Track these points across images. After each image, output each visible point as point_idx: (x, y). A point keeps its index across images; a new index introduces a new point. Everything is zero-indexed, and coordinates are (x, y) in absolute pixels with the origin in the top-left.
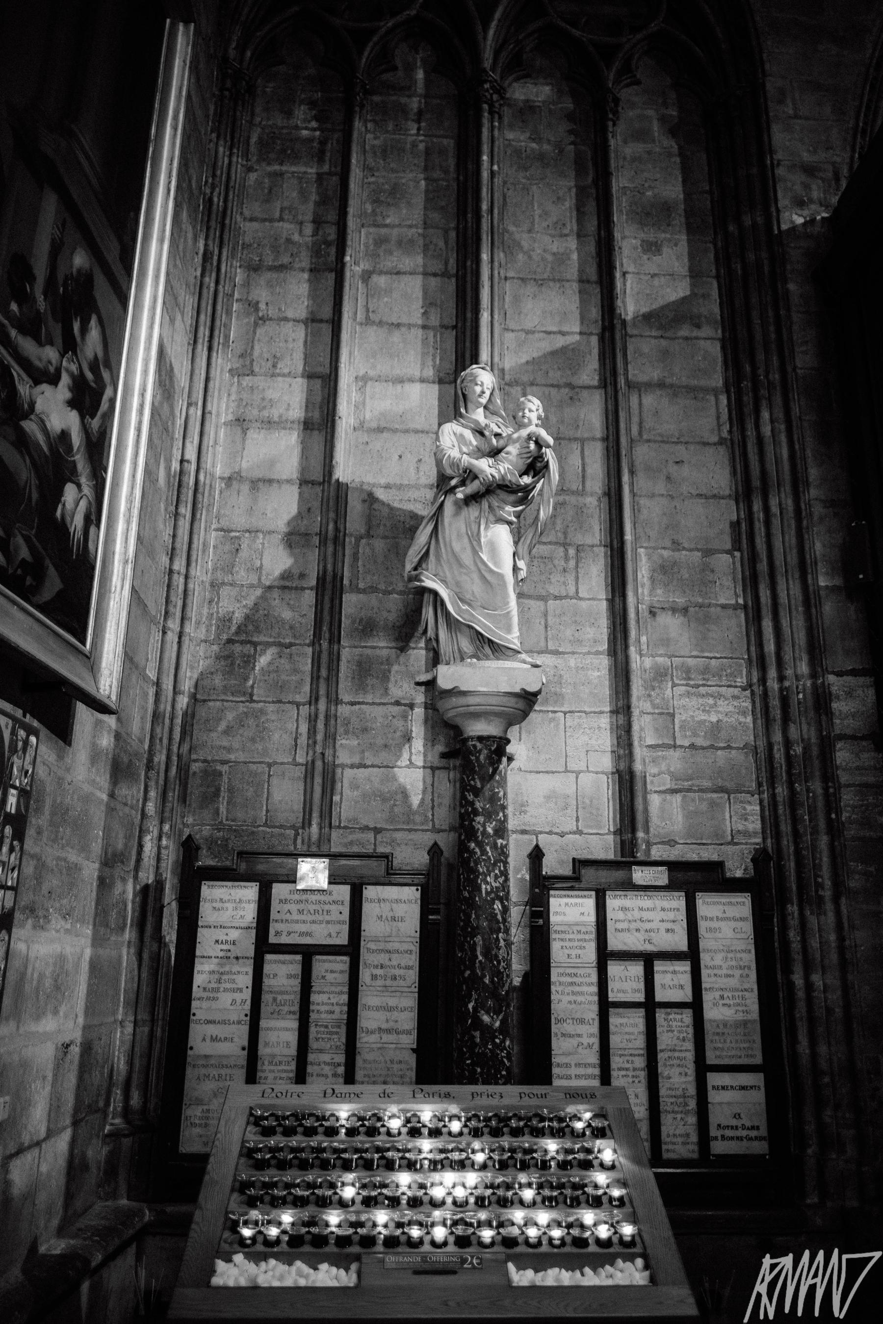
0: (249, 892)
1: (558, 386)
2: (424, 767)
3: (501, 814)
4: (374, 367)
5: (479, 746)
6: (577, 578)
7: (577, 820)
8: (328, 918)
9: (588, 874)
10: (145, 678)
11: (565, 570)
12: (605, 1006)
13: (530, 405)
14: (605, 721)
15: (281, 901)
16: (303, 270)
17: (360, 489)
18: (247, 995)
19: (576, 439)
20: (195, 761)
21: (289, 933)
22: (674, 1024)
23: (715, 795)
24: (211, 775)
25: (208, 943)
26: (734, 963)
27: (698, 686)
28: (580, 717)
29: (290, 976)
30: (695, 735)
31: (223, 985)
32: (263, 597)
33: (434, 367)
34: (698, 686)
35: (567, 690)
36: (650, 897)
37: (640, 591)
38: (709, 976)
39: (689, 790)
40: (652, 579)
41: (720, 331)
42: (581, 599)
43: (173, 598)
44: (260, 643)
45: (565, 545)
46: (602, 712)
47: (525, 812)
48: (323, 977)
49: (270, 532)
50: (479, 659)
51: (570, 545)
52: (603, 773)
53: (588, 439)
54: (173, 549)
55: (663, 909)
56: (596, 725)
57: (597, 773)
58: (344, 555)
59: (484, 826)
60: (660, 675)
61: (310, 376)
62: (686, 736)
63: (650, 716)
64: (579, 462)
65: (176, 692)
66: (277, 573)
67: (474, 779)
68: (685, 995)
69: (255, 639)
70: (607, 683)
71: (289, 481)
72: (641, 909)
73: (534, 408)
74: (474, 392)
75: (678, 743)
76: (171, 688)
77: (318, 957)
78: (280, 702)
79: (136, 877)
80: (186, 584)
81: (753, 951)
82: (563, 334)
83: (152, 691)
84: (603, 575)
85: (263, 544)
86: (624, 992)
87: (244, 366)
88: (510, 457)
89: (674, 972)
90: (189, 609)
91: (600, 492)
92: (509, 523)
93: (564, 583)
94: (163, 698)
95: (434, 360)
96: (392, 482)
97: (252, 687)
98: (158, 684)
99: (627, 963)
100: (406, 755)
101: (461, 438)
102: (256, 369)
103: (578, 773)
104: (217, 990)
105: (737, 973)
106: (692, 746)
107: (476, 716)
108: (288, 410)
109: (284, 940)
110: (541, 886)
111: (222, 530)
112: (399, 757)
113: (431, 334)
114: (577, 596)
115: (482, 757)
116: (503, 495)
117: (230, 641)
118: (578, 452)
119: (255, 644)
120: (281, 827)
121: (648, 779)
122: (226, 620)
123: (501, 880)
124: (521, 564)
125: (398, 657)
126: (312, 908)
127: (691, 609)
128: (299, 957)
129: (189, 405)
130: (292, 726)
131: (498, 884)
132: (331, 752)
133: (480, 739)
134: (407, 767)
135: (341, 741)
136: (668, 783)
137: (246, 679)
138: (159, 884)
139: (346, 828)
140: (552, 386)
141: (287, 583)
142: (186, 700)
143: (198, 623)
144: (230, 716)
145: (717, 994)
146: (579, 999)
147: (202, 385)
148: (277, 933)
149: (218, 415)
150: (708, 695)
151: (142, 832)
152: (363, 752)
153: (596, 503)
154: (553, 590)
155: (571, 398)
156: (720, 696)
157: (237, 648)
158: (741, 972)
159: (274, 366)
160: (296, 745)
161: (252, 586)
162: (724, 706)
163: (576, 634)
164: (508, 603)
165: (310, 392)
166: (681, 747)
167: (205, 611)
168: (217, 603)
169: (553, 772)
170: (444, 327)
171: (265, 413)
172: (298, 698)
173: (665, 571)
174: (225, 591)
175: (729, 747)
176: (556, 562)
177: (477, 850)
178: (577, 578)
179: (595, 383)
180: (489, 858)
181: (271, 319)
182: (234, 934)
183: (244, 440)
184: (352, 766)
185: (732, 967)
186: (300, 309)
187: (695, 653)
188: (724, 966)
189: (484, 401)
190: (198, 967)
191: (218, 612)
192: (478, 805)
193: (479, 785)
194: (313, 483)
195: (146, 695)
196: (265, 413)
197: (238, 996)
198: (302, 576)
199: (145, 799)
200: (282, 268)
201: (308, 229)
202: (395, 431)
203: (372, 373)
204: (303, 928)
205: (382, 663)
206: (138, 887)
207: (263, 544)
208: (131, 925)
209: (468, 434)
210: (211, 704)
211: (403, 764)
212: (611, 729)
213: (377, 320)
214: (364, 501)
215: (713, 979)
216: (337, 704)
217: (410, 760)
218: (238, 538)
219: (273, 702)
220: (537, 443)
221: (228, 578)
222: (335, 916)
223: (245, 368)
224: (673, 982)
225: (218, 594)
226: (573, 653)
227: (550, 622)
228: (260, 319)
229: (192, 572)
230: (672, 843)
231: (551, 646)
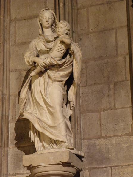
1: (104, 4)
6: (115, 99)
19: (112, 29)
28: (119, 169)
42: (116, 109)
46: (129, 165)
64: (114, 40)
114: (115, 108)
118: (114, 35)
140: (101, 4)
178: (115, 99)
226: (114, 136)
227: (102, 123)
231: (104, 134)
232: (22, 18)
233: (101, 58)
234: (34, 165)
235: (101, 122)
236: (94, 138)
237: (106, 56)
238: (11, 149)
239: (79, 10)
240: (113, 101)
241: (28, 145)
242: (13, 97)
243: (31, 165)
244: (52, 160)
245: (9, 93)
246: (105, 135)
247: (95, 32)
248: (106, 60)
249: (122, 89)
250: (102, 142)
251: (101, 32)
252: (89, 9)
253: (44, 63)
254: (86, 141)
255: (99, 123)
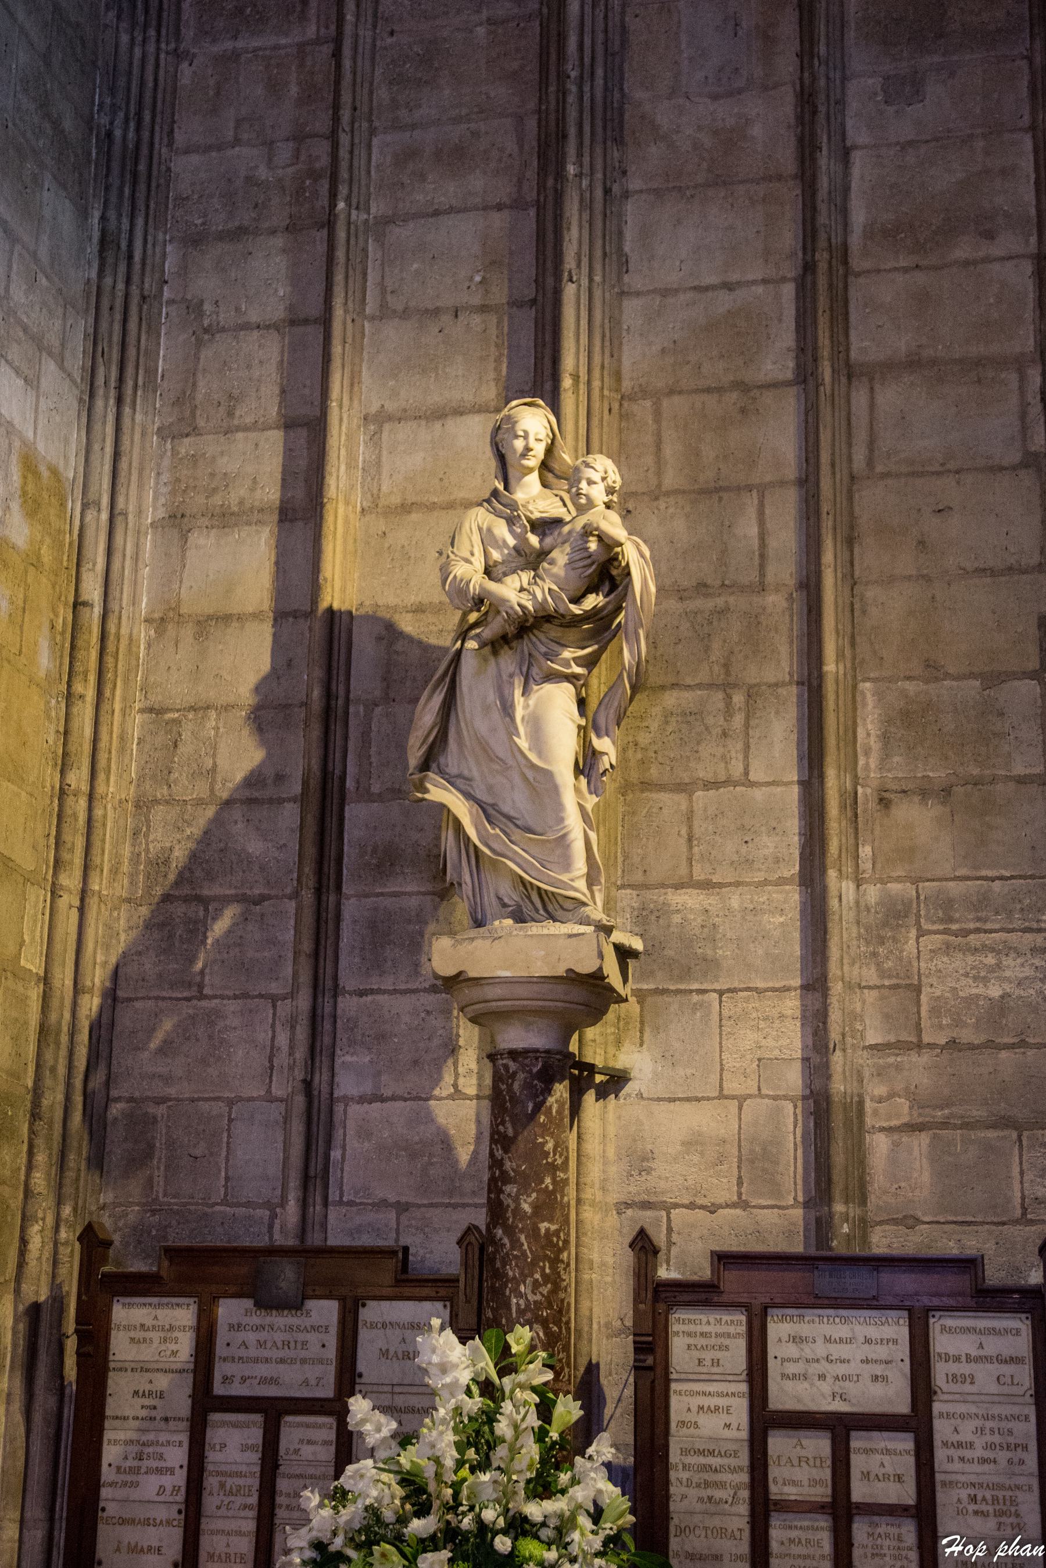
0: (182, 1315)
1: (720, 390)
2: (478, 1097)
3: (548, 1180)
4: (394, 394)
5: (513, 1066)
7: (740, 1183)
8: (303, 1354)
9: (732, 1279)
10: (20, 974)
11: (725, 734)
12: (763, 1507)
13: (589, 473)
14: (792, 1004)
15: (231, 1327)
16: (273, 232)
17: (372, 619)
18: (180, 1478)
19: (749, 488)
20: (118, 1099)
21: (244, 1379)
22: (887, 1543)
23: (991, 1134)
24: (141, 1124)
25: (122, 1397)
26: (997, 1439)
27: (966, 933)
28: (747, 1000)
29: (245, 1448)
30: (958, 1023)
31: (146, 1463)
32: (217, 821)
33: (497, 380)
34: (966, 933)
35: (725, 952)
36: (846, 1320)
37: (861, 762)
38: (950, 1459)
39: (944, 1125)
40: (885, 738)
41: (1033, 240)
42: (752, 784)
43: (67, 837)
44: (215, 898)
45: (727, 687)
46: (787, 989)
47: (649, 1171)
48: (297, 1451)
49: (227, 708)
50: (520, 918)
51: (735, 686)
52: (785, 1097)
53: (772, 484)
54: (65, 754)
55: (868, 1341)
56: (775, 1013)
57: (775, 1098)
58: (346, 738)
59: (517, 1200)
60: (896, 915)
61: (289, 425)
62: (941, 1027)
63: (874, 993)
64: (754, 531)
65: (77, 989)
66: (239, 777)
67: (503, 1123)
68: (906, 1493)
69: (206, 892)
70: (797, 935)
71: (256, 616)
72: (828, 1340)
73: (596, 477)
74: (515, 451)
75: (926, 1039)
76: (69, 983)
77: (289, 1419)
78: (245, 996)
79: (17, 1291)
80: (90, 809)
81: (1033, 1419)
82: (728, 287)
83: (35, 994)
84: (794, 737)
85: (217, 729)
86: (794, 1483)
87: (181, 420)
88: (555, 570)
89: (888, 1452)
90: (96, 850)
91: (791, 582)
92: (571, 678)
93: (723, 757)
94: (55, 1003)
95: (497, 369)
96: (426, 601)
97: (202, 972)
98: (46, 979)
99: (802, 1433)
100: (448, 1078)
101: (488, 538)
102: (201, 423)
103: (741, 1100)
104: (135, 1471)
105: (1003, 1456)
106: (953, 1044)
107: (504, 1016)
108: (252, 490)
109: (237, 1390)
110: (657, 1300)
111: (151, 710)
112: (437, 1081)
113: (494, 319)
115: (516, 1086)
116: (554, 631)
117: (166, 898)
118: (752, 512)
119: (204, 901)
120: (248, 1204)
121: (869, 1105)
122: (162, 862)
123: (545, 1290)
124: (603, 744)
125: (436, 908)
126: (279, 1337)
127: (959, 790)
128: (258, 1418)
129: (85, 506)
130: (263, 1036)
131: (538, 1297)
132: (325, 1077)
133: (514, 1054)
134: (451, 1097)
135: (343, 1058)
136: (903, 1111)
137: (192, 960)
138: (58, 1301)
139: (351, 1203)
140: (708, 390)
141: (256, 793)
142: (96, 1001)
143: (115, 871)
144: (168, 1025)
145: (964, 1494)
146: (719, 1494)
147: (107, 468)
148: (226, 1379)
149: (140, 512)
150: (985, 948)
151: (26, 1220)
152: (379, 1073)
153: (785, 604)
154: (703, 772)
155: (743, 411)
156: (1009, 949)
157: (179, 910)
158: (1009, 1455)
159: (230, 414)
160: (272, 1068)
161: (200, 802)
162: (1015, 968)
163: (744, 849)
164: (562, 820)
165: (289, 453)
166: (931, 1046)
167: (127, 851)
168: (146, 836)
169: (698, 1099)
170: (515, 303)
171: (217, 500)
172: (275, 988)
173: (908, 722)
174: (158, 813)
175: (1023, 1044)
176: (710, 721)
177: (506, 1241)
178: (747, 747)
179: (789, 375)
180: (524, 1253)
181: (223, 330)
182: (162, 1382)
183: (184, 551)
184: (362, 1100)
185: (991, 1446)
186: (273, 304)
187: (962, 872)
188: (979, 1442)
189: (533, 462)
190: (108, 1435)
191: (147, 851)
192: (508, 1165)
193: (510, 1132)
194: (295, 614)
195: (22, 1001)
196: (217, 500)
197: (167, 1481)
198: (280, 778)
199: (30, 1167)
200: (239, 233)
201: (284, 152)
202: (432, 507)
203: (391, 406)
204: (263, 1370)
205: (409, 922)
206: (21, 1308)
207: (217, 729)
208: (12, 1368)
209: (501, 530)
210: (138, 1004)
211: (444, 1094)
212: (804, 1017)
213: (400, 308)
214: (379, 638)
215: (957, 1466)
216: (335, 996)
217: (455, 1086)
218: (177, 722)
219: (236, 997)
220: (600, 539)
221: (163, 792)
222: (314, 1350)
223: (182, 426)
224: (882, 1469)
225: (148, 821)
226: (737, 884)
227: (697, 832)
228: (206, 331)
229: (101, 789)
230: (910, 1222)
231: (699, 873)
232: (405, 410)
233: (702, 588)
234: (472, 974)
235: (690, 827)
236: (663, 886)
237: (723, 585)
238: (353, 900)
239: (626, 404)
240: (741, 757)
241: (416, 889)
242: (361, 709)
243: (460, 973)
244: (539, 963)
245: (348, 691)
246: (702, 877)
247: (684, 492)
248: (720, 602)
249: (777, 713)
250: (689, 900)
251: (706, 492)
252: (665, 403)
253: (519, 605)
254: (635, 893)
255: (684, 832)
